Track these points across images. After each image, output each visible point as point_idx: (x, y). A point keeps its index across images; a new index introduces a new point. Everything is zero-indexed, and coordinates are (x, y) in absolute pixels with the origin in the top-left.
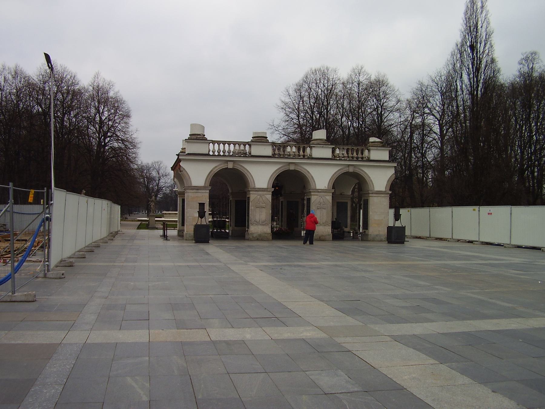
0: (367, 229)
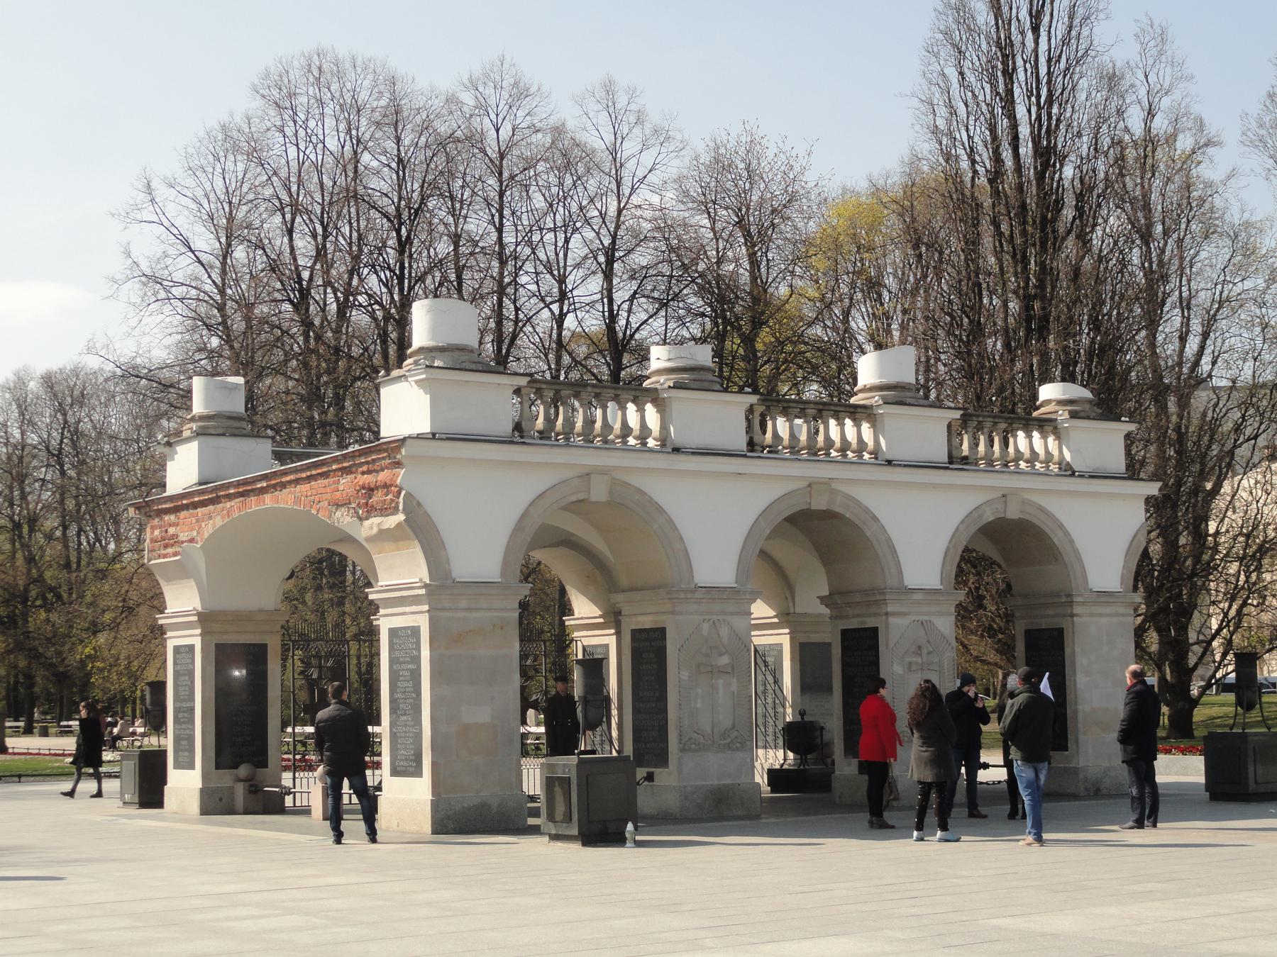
0: (1065, 748)
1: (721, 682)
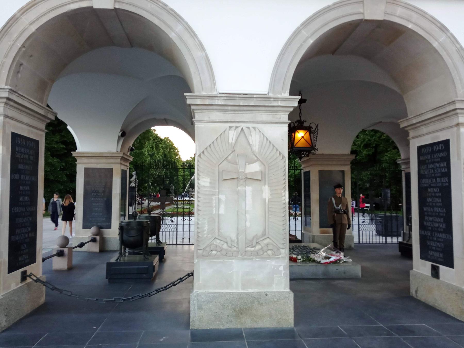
1: (249, 189)
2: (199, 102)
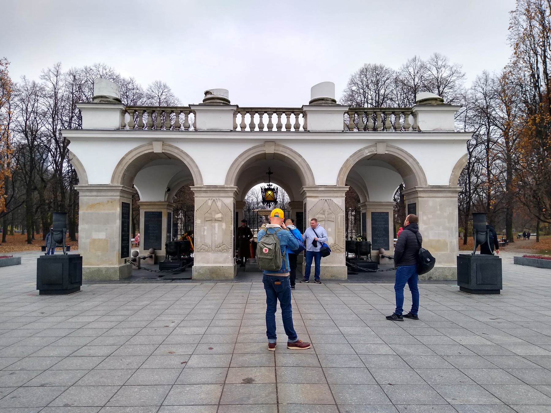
1: (217, 224)
2: (196, 189)
